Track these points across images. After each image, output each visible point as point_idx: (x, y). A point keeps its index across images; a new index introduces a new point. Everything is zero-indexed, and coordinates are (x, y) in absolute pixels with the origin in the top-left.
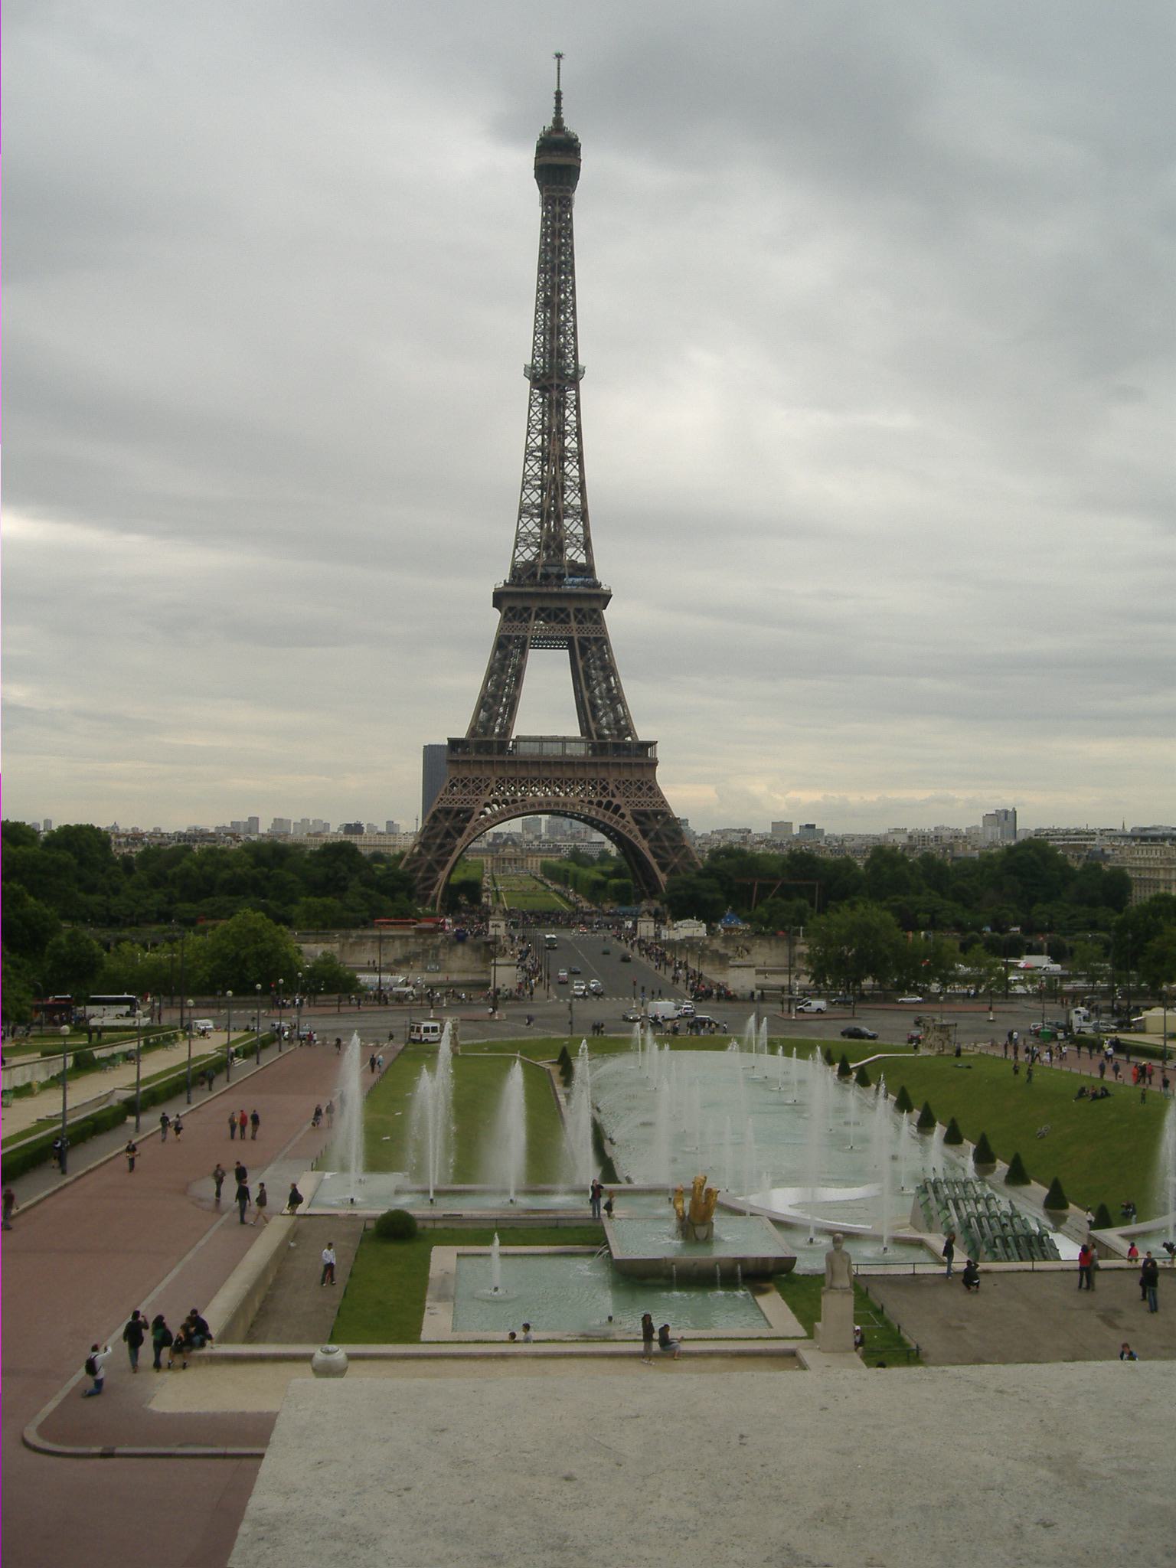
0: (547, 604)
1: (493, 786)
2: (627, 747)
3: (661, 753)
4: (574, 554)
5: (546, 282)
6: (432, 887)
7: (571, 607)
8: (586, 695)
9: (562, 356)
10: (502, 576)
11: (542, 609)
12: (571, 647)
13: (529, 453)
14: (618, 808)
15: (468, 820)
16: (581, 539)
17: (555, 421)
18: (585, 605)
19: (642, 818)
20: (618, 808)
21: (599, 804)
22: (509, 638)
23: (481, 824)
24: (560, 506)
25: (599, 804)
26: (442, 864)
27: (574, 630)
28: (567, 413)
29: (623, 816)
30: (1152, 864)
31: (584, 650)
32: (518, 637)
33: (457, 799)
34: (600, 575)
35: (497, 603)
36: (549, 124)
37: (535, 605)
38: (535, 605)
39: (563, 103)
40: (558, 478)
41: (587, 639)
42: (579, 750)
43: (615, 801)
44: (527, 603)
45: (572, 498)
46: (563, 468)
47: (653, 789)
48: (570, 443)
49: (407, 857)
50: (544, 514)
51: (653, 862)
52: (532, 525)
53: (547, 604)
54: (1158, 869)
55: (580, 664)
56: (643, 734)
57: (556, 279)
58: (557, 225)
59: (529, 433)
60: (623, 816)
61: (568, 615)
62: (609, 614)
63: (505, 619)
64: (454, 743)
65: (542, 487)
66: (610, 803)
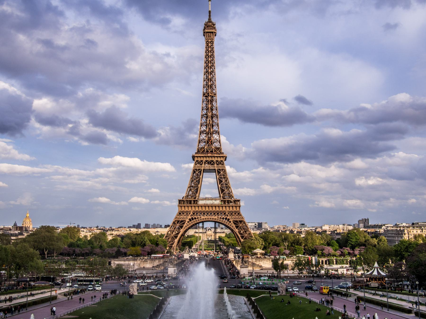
0: (208, 159)
1: (192, 213)
3: (242, 204)
4: (217, 145)
5: (207, 66)
6: (173, 244)
7: (215, 160)
8: (219, 186)
9: (211, 86)
11: (206, 161)
12: (215, 172)
13: (202, 116)
14: (229, 219)
15: (184, 224)
16: (218, 140)
17: (210, 106)
18: (219, 159)
19: (236, 222)
20: (229, 219)
21: (226, 219)
22: (196, 169)
23: (188, 225)
24: (212, 130)
25: (223, 218)
26: (176, 237)
27: (216, 167)
28: (214, 104)
29: (230, 222)
30: (393, 235)
31: (219, 172)
32: (199, 169)
33: (182, 217)
34: (222, 151)
35: (194, 160)
36: (207, 20)
38: (205, 159)
39: (211, 14)
40: (211, 122)
41: (220, 170)
42: (218, 202)
43: (228, 218)
44: (202, 159)
45: (215, 128)
46: (212, 119)
48: (214, 112)
49: (166, 235)
51: (239, 236)
53: (208, 159)
54: (395, 237)
55: (218, 177)
56: (235, 198)
57: (210, 65)
58: (210, 49)
59: (203, 110)
60: (230, 222)
61: (214, 163)
64: (180, 201)
65: (206, 125)
66: (226, 219)
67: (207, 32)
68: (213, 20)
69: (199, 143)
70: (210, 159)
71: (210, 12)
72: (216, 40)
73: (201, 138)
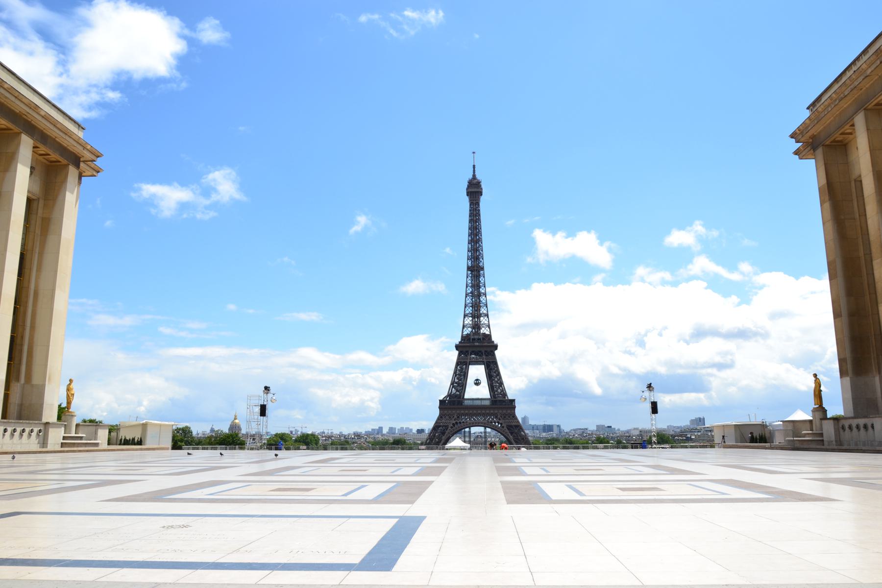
2: (504, 401)
4: (484, 330)
7: (483, 350)
10: (458, 340)
13: (467, 295)
19: (509, 427)
36: (471, 177)
37: (470, 350)
38: (470, 350)
42: (487, 403)
44: (467, 349)
45: (483, 310)
47: (514, 416)
50: (473, 317)
52: (469, 321)
56: (510, 397)
62: (497, 353)
63: (459, 355)
67: (471, 192)
68: (478, 177)
69: (464, 327)
70: (479, 349)
71: (474, 166)
72: (484, 200)
73: (466, 322)
